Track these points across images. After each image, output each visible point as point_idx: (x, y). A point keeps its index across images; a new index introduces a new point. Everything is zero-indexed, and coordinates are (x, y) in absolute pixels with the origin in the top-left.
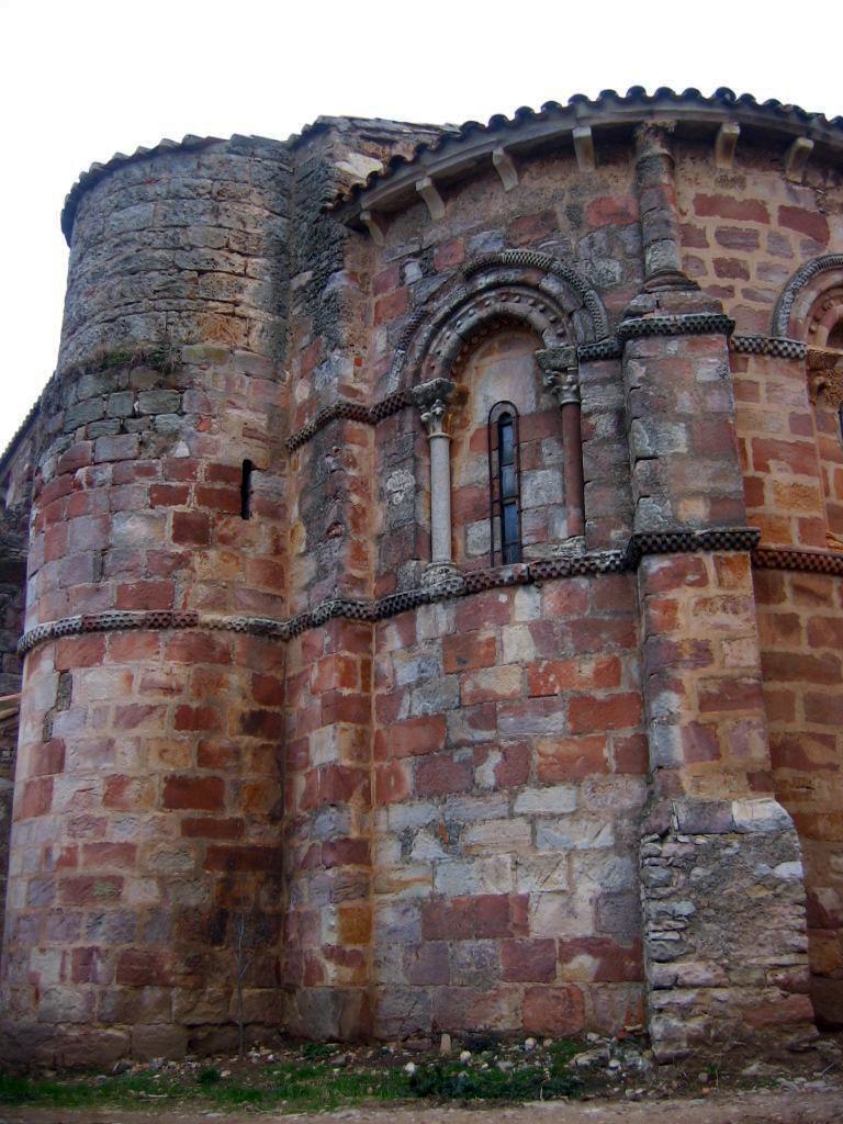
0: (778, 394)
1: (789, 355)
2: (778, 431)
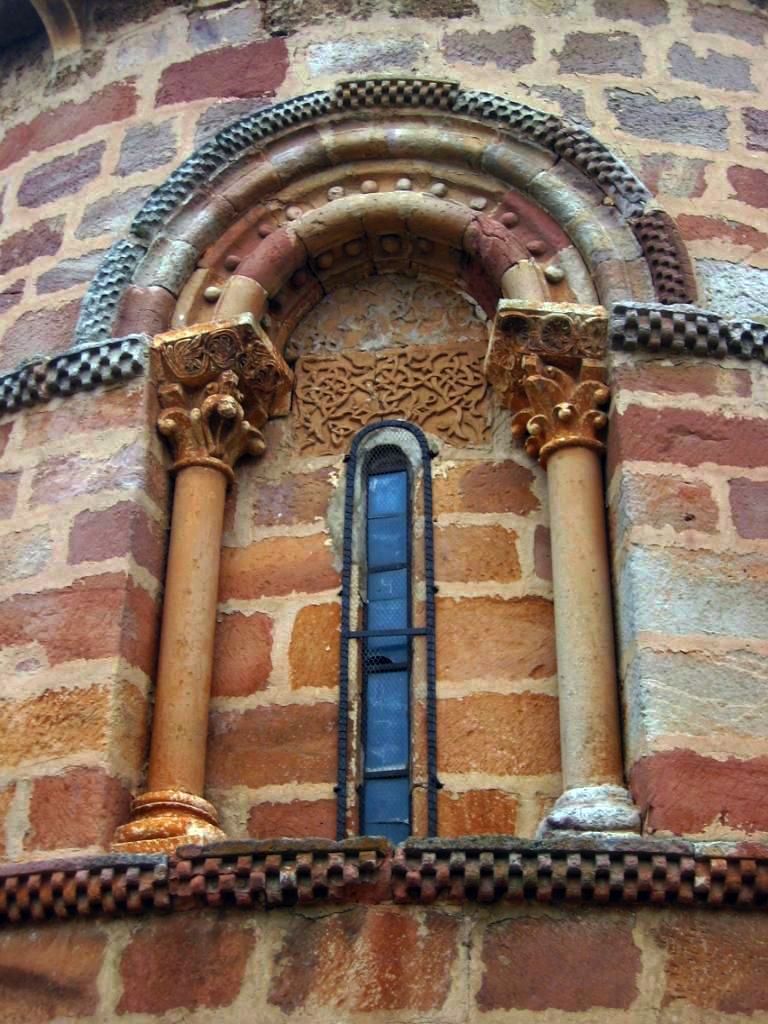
0: (60, 479)
1: (97, 379)
2: (40, 567)
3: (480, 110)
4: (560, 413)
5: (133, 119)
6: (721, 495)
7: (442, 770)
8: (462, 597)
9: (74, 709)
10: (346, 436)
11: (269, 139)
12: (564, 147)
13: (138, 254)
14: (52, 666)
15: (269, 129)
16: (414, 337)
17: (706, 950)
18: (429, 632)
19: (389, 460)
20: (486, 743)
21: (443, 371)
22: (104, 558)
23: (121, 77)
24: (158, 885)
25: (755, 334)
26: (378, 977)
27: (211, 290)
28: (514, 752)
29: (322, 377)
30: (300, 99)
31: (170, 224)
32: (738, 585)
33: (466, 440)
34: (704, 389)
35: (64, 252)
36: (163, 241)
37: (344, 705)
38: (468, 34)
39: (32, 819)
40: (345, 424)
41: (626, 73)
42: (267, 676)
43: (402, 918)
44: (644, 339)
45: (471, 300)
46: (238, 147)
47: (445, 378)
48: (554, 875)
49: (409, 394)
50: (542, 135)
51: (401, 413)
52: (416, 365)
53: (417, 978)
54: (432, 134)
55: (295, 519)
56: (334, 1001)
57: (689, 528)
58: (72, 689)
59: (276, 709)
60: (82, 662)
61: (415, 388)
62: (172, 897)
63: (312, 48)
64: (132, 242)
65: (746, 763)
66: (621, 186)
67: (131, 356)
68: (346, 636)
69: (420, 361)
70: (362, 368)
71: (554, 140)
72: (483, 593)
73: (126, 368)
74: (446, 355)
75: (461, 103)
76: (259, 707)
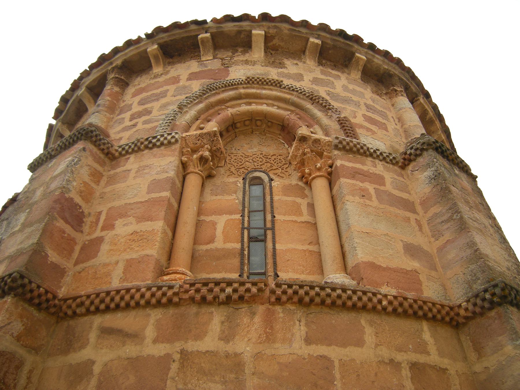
3: (289, 88)
4: (317, 166)
5: (179, 84)
6: (372, 191)
7: (279, 272)
8: (284, 220)
9: (145, 237)
10: (243, 173)
11: (223, 89)
12: (315, 100)
13: (179, 114)
14: (137, 224)
15: (224, 86)
16: (266, 150)
17: (388, 329)
18: (273, 229)
19: (257, 181)
20: (294, 264)
21: (275, 159)
22: (160, 192)
23: (175, 75)
24: (176, 294)
25: (377, 151)
26: (264, 331)
27: (202, 126)
28: (304, 267)
29: (235, 157)
30: (234, 79)
31: (190, 107)
32: (381, 216)
33: (283, 177)
34: (363, 164)
35: (152, 115)
36: (187, 111)
37: (242, 249)
38: (284, 73)
39: (123, 273)
40: (243, 170)
41: (330, 88)
42: (215, 239)
43: (273, 310)
44: (344, 147)
45: (283, 142)
46: (214, 89)
47: (275, 161)
48: (332, 296)
49: (264, 164)
50: (309, 96)
51: (261, 168)
52: (265, 157)
53: (280, 332)
54: (275, 93)
55: (225, 194)
56: (246, 339)
57: (364, 198)
58: (145, 231)
59: (217, 250)
60: (150, 222)
61: (266, 162)
62: (180, 299)
63: (237, 71)
64: (177, 110)
65: (392, 268)
66: (334, 110)
67: (175, 137)
68: (243, 229)
69: (267, 156)
70: (248, 156)
71: (312, 98)
72: (290, 219)
73: (173, 140)
74: (276, 155)
75: (283, 86)
76: (211, 248)
